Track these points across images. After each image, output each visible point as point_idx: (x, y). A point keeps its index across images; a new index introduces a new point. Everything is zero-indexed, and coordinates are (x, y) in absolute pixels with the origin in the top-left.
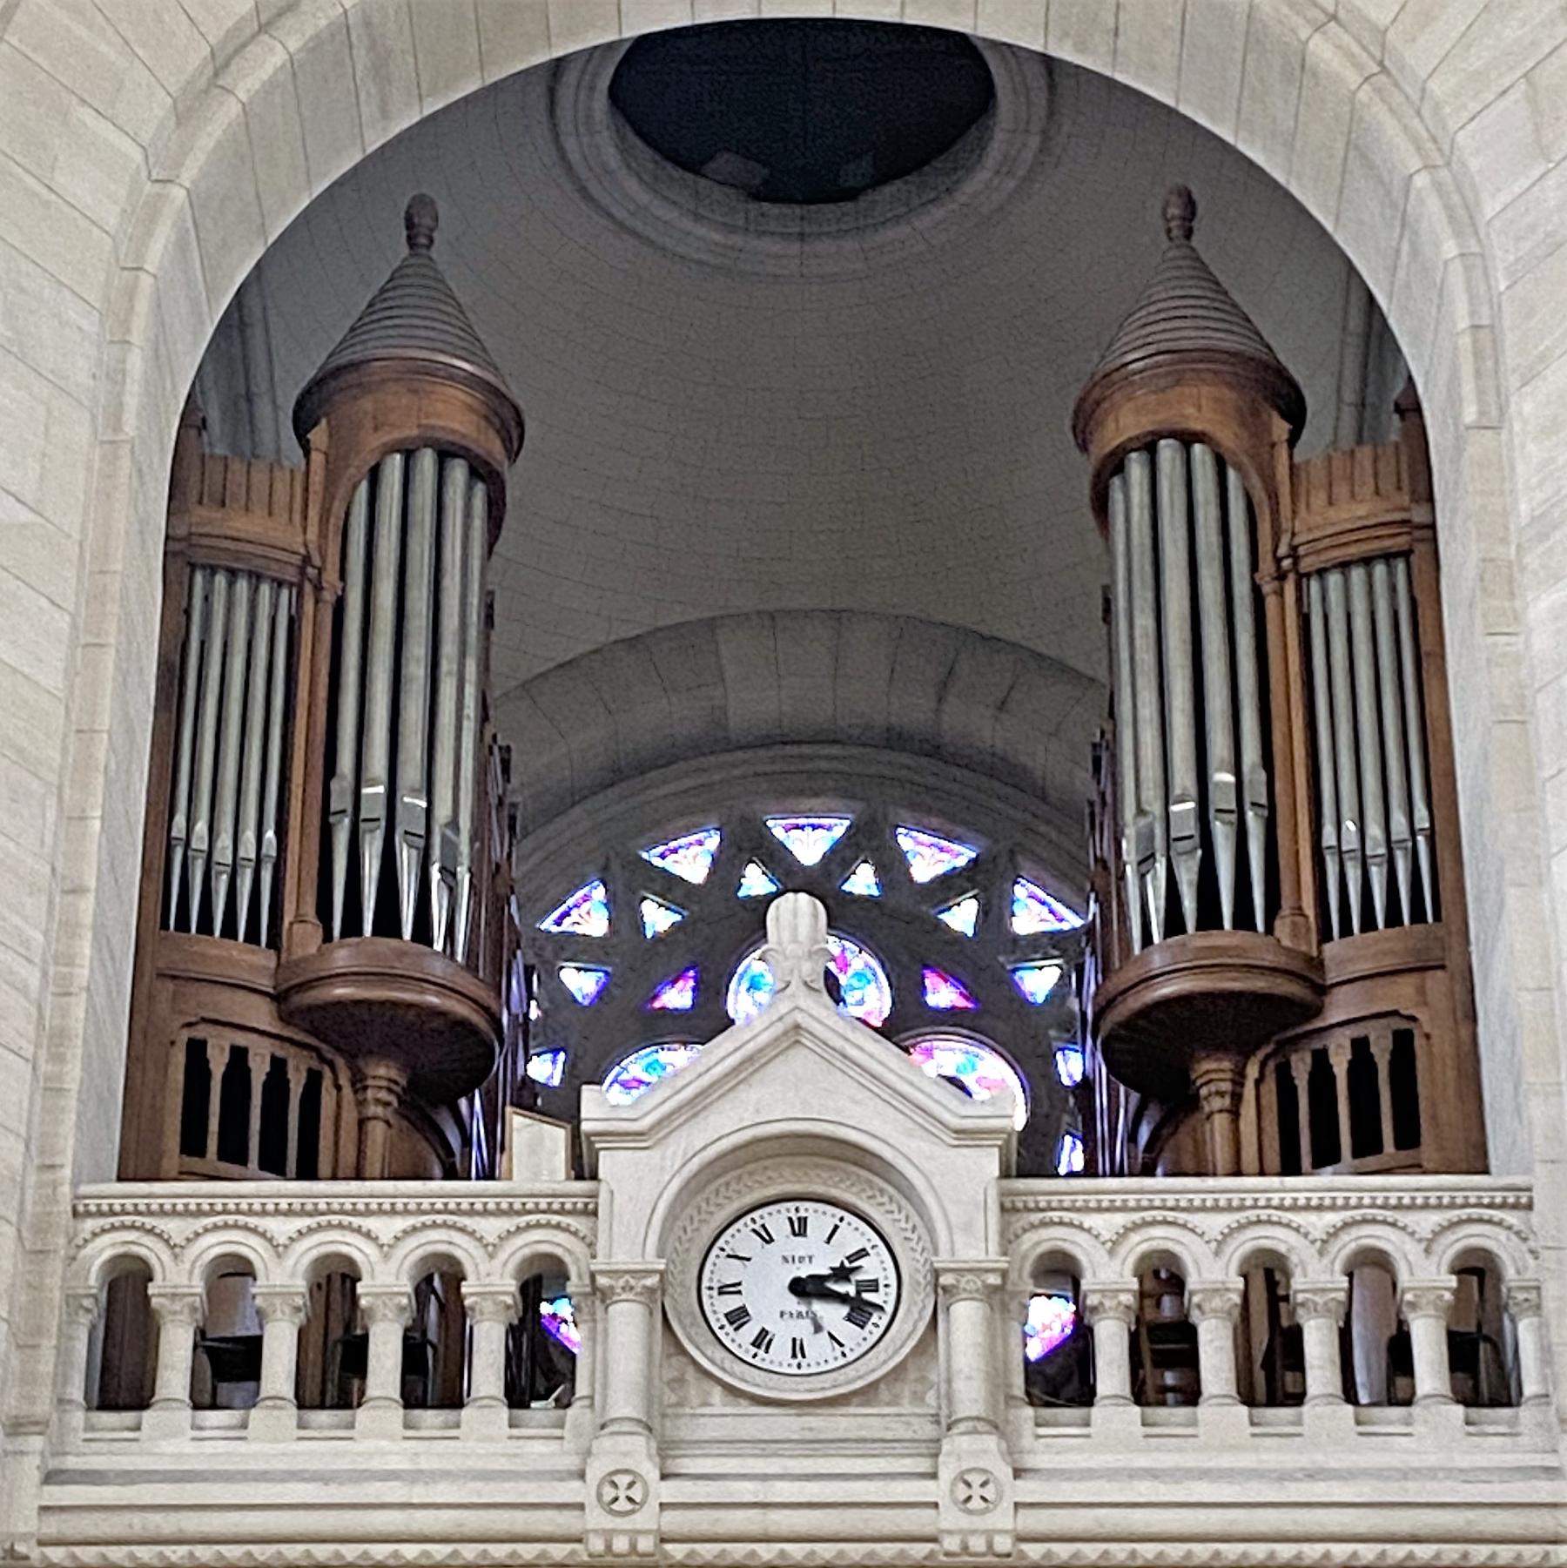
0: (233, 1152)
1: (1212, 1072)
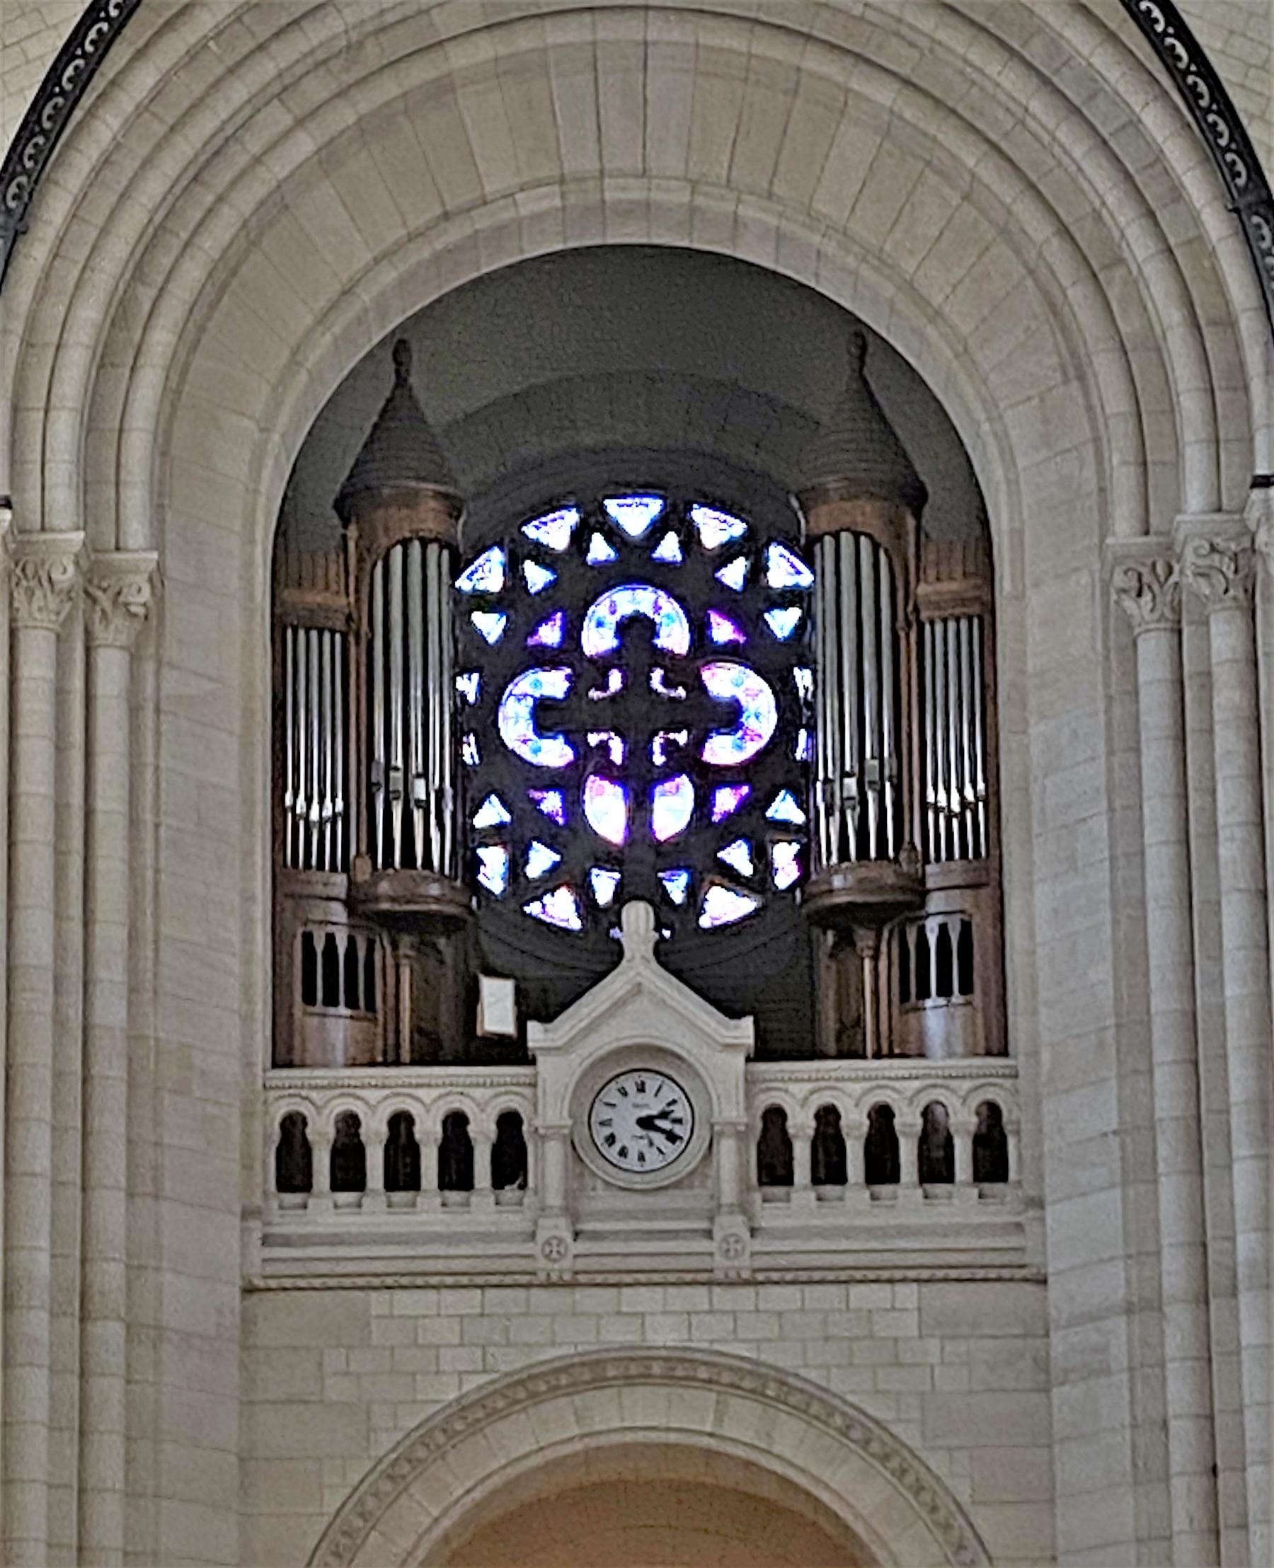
0: (331, 1000)
1: (864, 939)
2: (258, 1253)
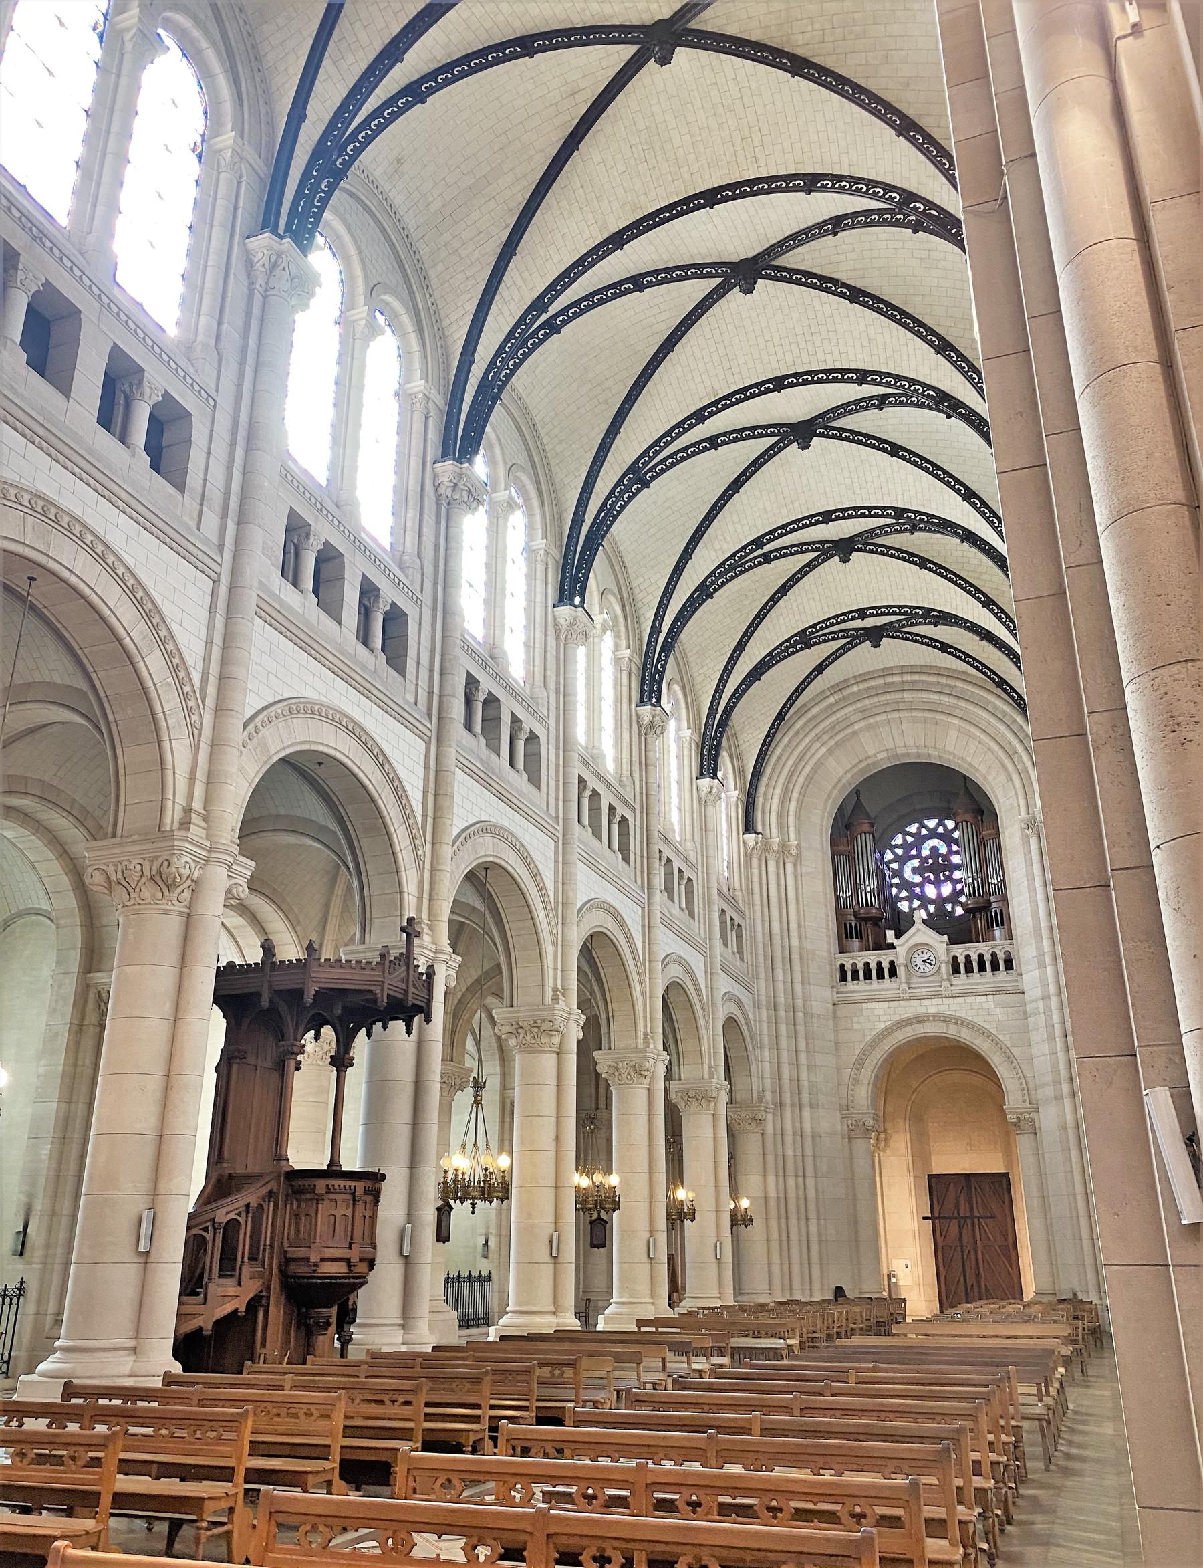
1: (978, 915)
2: (835, 995)
